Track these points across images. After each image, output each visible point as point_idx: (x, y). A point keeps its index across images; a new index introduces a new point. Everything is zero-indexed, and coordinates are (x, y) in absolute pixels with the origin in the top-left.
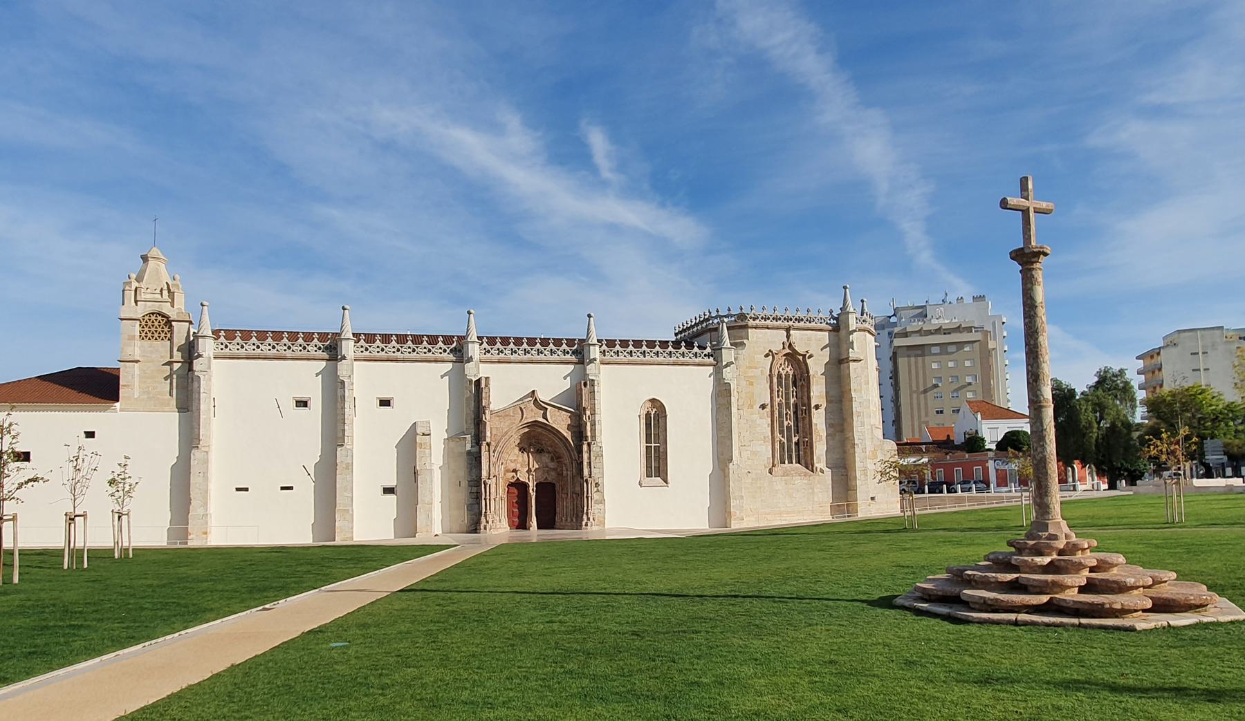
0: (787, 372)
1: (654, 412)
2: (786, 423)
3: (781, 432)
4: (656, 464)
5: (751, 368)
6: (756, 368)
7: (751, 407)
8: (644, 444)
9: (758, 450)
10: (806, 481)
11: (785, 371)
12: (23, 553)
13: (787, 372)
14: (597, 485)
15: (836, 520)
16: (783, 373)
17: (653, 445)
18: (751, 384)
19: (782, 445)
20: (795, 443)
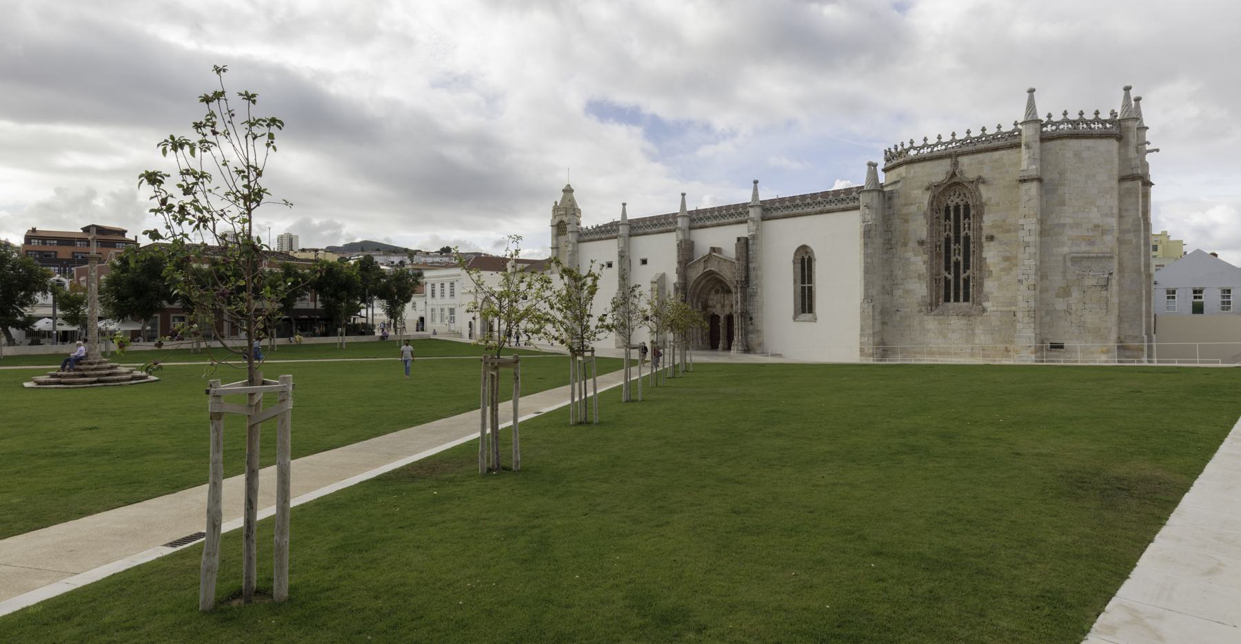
0: (957, 203)
1: (807, 257)
2: (953, 259)
3: (947, 269)
4: (805, 303)
5: (906, 205)
6: (912, 204)
7: (905, 245)
8: (799, 285)
9: (911, 288)
10: (965, 322)
11: (954, 203)
12: (278, 345)
13: (957, 203)
14: (751, 319)
15: (864, 362)
16: (952, 205)
17: (806, 285)
18: (907, 221)
19: (947, 282)
20: (964, 279)
